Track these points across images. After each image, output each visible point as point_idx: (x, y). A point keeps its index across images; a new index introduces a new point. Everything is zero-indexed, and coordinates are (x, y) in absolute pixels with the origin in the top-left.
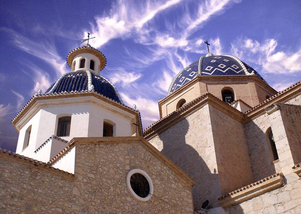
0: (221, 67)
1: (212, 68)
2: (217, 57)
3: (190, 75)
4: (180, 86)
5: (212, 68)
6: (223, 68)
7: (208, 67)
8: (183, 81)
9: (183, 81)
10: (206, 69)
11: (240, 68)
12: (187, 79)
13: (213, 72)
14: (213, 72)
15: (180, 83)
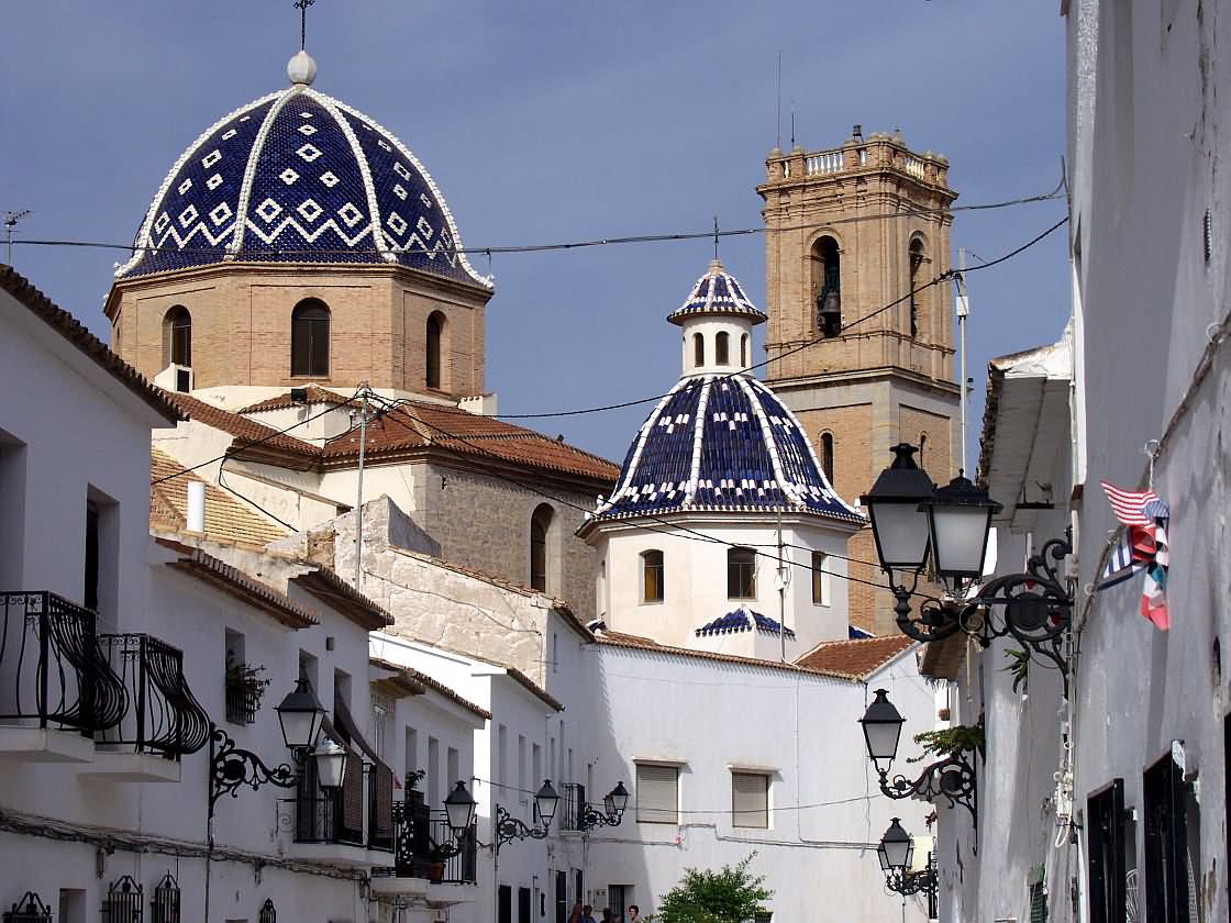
0: (306, 215)
1: (279, 209)
2: (309, 153)
3: (213, 215)
4: (181, 244)
5: (279, 209)
6: (311, 218)
7: (265, 204)
8: (191, 227)
9: (191, 227)
10: (260, 211)
11: (367, 219)
12: (202, 226)
13: (275, 234)
14: (275, 234)
15: (183, 233)
